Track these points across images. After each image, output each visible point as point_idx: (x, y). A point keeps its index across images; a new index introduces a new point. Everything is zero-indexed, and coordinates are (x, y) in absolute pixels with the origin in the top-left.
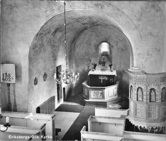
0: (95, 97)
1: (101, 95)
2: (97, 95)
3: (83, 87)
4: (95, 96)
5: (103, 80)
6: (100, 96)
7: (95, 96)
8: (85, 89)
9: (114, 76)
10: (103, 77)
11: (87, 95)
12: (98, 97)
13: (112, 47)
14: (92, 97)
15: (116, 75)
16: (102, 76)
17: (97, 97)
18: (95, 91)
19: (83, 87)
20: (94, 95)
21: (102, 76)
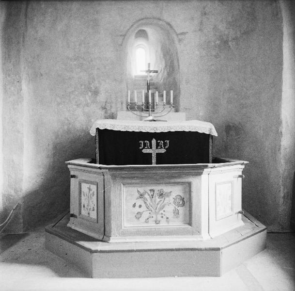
0: (141, 224)
1: (176, 213)
2: (156, 213)
3: (72, 180)
4: (143, 219)
5: (157, 154)
6: (170, 215)
7: (146, 215)
8: (85, 187)
9: (206, 137)
10: (158, 145)
11: (94, 215)
12: (163, 224)
13: (180, 40)
14: (126, 225)
15: (215, 134)
16: (154, 141)
17: (157, 222)
18: (142, 190)
19: (72, 180)
20: (137, 209)
21: (154, 141)
